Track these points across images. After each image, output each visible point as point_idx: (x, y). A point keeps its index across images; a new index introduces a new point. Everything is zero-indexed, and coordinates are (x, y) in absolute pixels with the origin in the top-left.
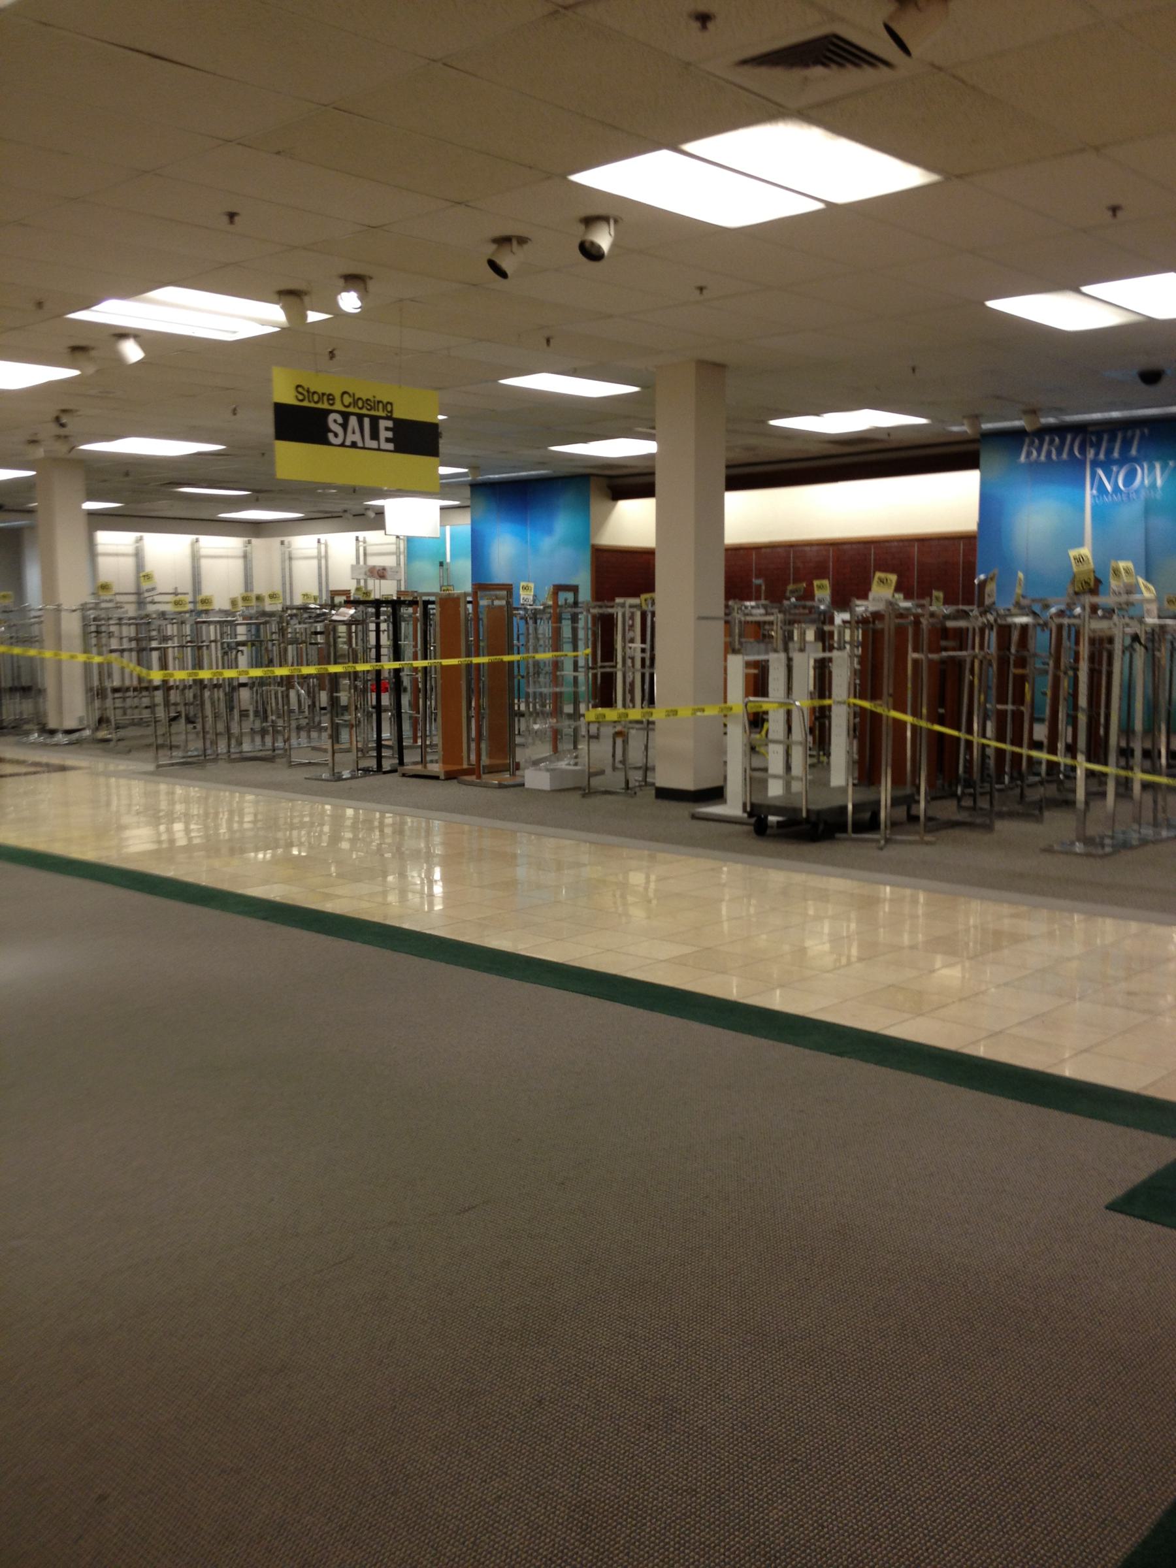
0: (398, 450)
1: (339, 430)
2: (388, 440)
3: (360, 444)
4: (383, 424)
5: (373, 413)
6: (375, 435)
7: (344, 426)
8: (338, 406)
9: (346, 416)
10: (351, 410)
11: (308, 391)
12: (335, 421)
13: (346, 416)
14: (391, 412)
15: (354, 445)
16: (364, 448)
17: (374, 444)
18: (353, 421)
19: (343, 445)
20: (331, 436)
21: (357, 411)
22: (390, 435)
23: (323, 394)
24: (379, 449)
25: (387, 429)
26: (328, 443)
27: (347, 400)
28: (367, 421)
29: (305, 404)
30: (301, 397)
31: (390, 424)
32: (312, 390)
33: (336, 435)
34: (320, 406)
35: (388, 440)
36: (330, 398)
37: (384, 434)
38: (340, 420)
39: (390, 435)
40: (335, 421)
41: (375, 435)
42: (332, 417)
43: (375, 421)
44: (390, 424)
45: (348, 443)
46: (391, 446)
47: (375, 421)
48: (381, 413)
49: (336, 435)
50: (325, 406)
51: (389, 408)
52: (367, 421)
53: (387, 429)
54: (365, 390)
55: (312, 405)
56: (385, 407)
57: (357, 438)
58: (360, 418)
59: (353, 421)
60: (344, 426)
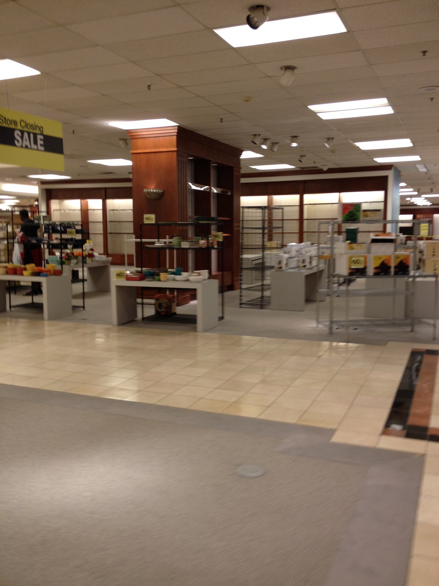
2: (41, 145)
3: (29, 146)
4: (39, 137)
6: (36, 143)
7: (22, 137)
8: (19, 127)
12: (18, 135)
13: (22, 132)
14: (42, 132)
15: (27, 147)
17: (35, 147)
18: (26, 135)
19: (22, 147)
20: (16, 142)
21: (27, 130)
24: (38, 149)
25: (41, 140)
26: (14, 145)
28: (32, 136)
32: (6, 118)
33: (18, 141)
35: (41, 145)
36: (15, 123)
37: (40, 142)
38: (20, 134)
40: (18, 135)
41: (36, 143)
43: (35, 135)
45: (24, 145)
46: (42, 148)
47: (35, 135)
49: (18, 141)
50: (13, 126)
52: (32, 136)
53: (41, 140)
54: (31, 120)
55: (7, 126)
56: (40, 129)
57: (28, 144)
58: (29, 133)
59: (26, 135)
60: (22, 137)
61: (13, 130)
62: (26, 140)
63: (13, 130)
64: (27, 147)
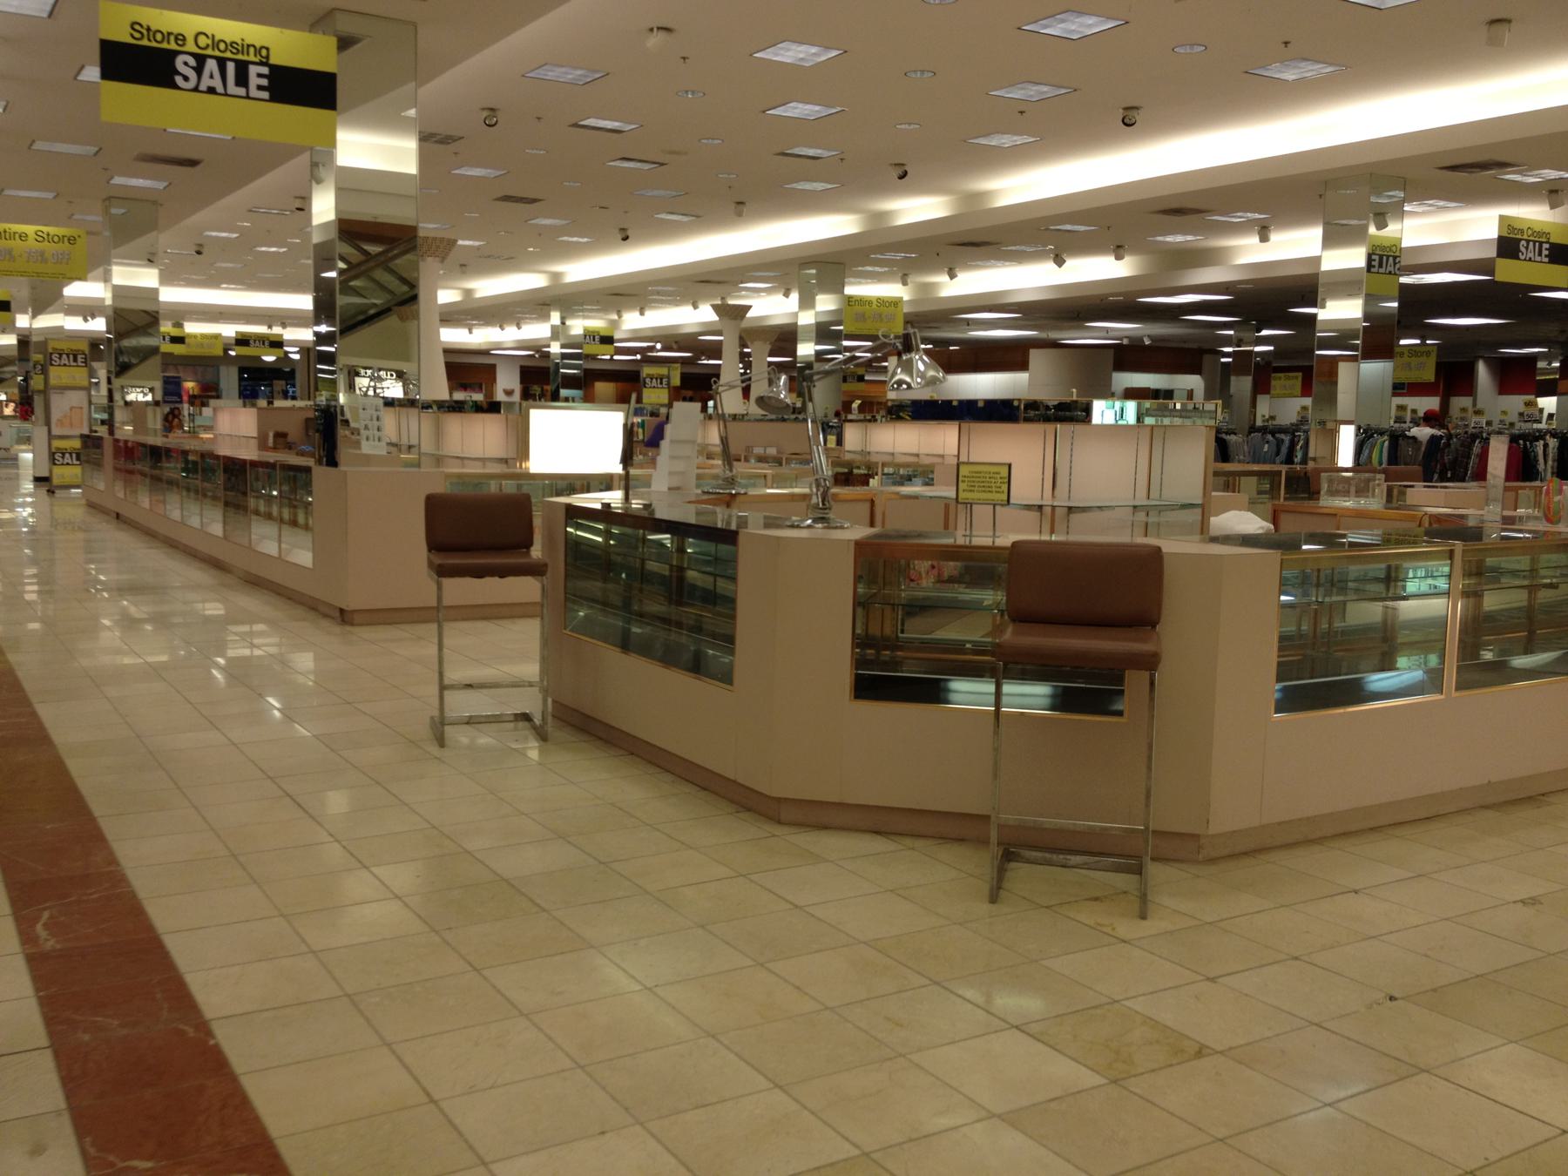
0: (273, 99)
1: (192, 75)
2: (260, 88)
3: (220, 89)
4: (253, 70)
5: (240, 57)
6: (242, 80)
7: (199, 70)
9: (201, 60)
10: (209, 52)
11: (149, 29)
12: (186, 64)
13: (201, 60)
14: (267, 57)
15: (211, 90)
16: (226, 95)
17: (241, 91)
18: (211, 65)
19: (196, 89)
20: (179, 80)
21: (217, 53)
22: (264, 82)
23: (169, 34)
24: (248, 97)
25: (260, 75)
26: (175, 86)
27: (203, 41)
28: (231, 67)
29: (145, 42)
30: (137, 35)
31: (265, 70)
32: (153, 28)
33: (186, 79)
34: (165, 45)
35: (260, 88)
37: (254, 81)
38: (192, 62)
39: (264, 82)
40: (186, 64)
42: (179, 60)
43: (242, 68)
44: (265, 70)
45: (203, 87)
46: (266, 95)
47: (242, 68)
48: (252, 58)
49: (186, 79)
50: (173, 46)
51: (264, 52)
52: (231, 67)
53: (260, 75)
55: (154, 44)
57: (217, 83)
58: (222, 63)
59: (211, 65)
60: (199, 70)
61: (174, 54)
62: (211, 77)
63: (174, 54)
64: (211, 90)
